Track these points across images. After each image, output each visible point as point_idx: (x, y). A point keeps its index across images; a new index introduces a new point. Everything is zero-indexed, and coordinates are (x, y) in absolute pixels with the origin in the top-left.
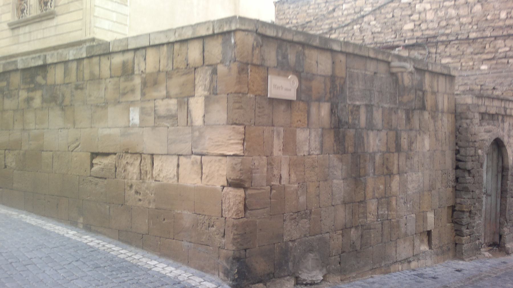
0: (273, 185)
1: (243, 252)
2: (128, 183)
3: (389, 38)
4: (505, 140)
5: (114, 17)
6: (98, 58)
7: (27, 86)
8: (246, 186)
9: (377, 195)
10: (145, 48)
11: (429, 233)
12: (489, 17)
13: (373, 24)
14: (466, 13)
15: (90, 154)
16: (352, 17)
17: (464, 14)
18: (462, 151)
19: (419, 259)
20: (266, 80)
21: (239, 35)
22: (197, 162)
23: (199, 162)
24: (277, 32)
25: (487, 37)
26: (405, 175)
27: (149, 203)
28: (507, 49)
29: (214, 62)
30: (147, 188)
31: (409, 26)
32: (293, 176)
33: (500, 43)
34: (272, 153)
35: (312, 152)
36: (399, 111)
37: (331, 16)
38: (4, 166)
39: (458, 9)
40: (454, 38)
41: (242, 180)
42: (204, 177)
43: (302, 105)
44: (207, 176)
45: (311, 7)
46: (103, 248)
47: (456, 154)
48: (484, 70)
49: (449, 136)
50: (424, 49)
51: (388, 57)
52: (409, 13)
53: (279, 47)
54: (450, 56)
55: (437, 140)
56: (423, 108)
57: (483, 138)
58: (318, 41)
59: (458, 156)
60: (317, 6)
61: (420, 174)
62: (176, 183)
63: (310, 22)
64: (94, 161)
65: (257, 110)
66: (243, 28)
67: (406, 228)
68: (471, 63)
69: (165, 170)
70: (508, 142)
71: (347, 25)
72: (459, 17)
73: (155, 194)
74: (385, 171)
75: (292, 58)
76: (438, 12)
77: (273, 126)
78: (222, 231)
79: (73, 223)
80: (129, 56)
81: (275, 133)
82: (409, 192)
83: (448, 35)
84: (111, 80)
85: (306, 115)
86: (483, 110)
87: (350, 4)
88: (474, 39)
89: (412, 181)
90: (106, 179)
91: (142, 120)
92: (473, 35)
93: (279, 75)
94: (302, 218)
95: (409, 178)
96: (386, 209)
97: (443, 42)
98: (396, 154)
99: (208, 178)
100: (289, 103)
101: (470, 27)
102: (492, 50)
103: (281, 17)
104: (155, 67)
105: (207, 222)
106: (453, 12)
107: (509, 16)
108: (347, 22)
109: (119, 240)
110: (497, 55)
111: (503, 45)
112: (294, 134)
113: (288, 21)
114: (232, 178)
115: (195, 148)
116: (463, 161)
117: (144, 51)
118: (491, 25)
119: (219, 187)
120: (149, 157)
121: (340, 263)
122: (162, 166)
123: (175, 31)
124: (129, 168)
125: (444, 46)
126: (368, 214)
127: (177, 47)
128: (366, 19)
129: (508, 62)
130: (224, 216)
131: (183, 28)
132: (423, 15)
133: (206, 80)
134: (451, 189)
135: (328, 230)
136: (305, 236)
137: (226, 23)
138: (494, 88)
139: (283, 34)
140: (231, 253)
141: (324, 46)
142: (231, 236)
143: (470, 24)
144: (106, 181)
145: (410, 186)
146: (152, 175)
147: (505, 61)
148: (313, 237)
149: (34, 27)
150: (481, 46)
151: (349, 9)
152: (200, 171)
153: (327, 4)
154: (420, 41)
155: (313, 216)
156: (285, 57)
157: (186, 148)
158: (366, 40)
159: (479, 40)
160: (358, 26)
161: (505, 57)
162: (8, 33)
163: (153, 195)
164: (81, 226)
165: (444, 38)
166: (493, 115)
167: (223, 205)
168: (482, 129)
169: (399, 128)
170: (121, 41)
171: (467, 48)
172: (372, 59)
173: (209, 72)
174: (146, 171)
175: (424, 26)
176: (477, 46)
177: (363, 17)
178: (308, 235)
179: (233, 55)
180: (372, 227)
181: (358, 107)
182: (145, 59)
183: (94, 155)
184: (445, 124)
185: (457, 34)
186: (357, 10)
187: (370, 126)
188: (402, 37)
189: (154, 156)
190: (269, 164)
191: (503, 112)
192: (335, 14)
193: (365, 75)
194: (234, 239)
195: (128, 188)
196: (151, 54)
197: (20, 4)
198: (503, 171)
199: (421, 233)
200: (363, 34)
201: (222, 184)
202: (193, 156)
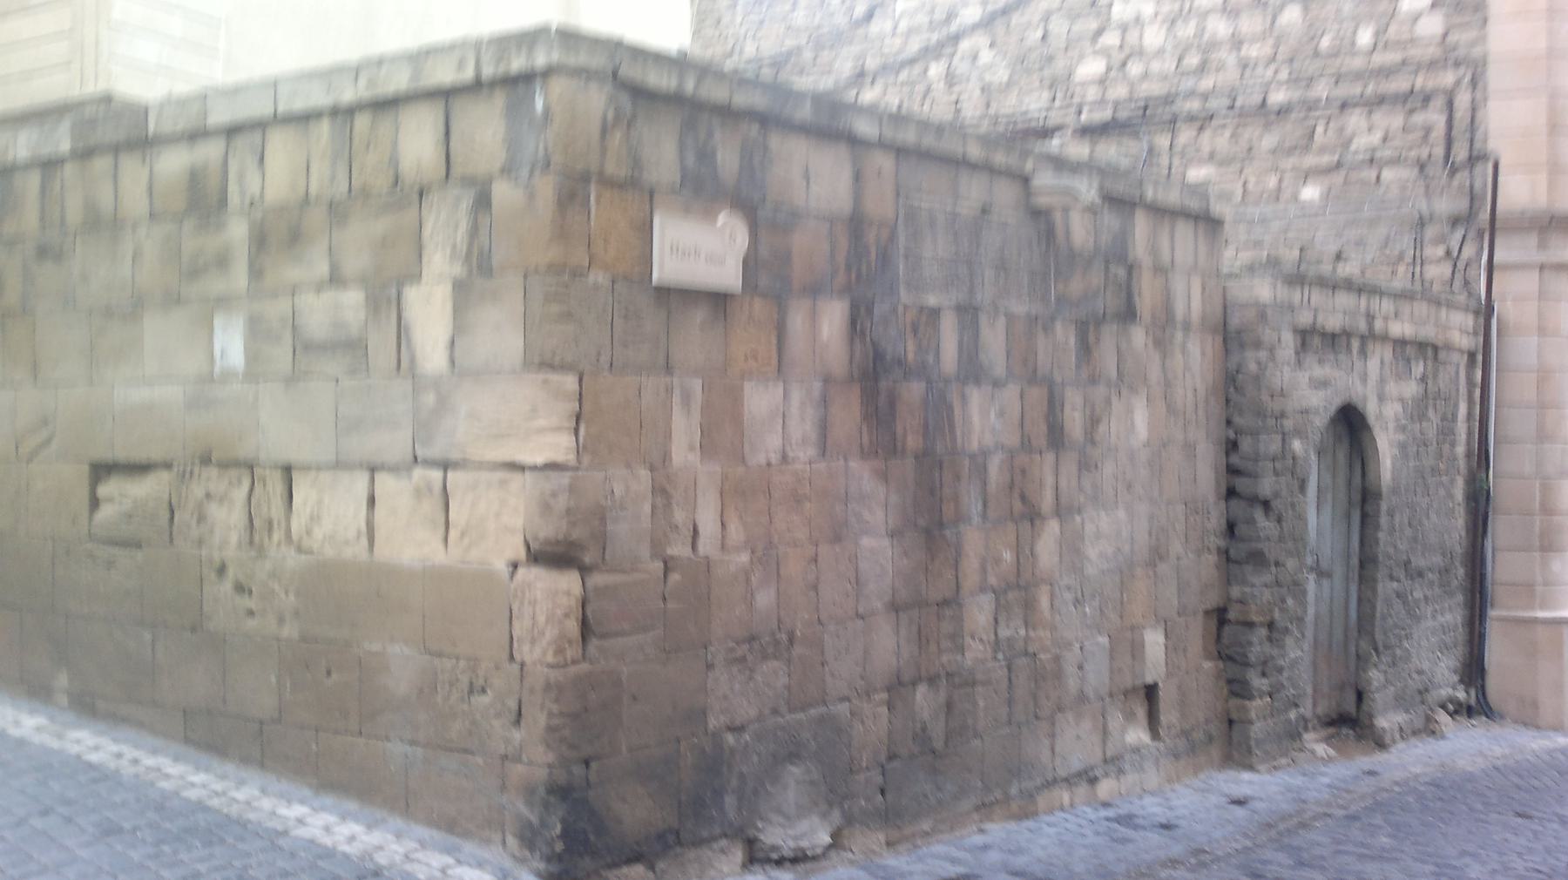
0: (672, 558)
1: (578, 770)
3: (1034, 103)
4: (1371, 409)
9: (992, 580)
10: (260, 126)
11: (1151, 692)
13: (986, 61)
15: (86, 468)
18: (1246, 444)
19: (1121, 772)
20: (646, 230)
21: (558, 86)
22: (430, 490)
23: (438, 486)
26: (1078, 519)
27: (281, 620)
30: (273, 575)
31: (1091, 68)
34: (666, 457)
35: (791, 454)
36: (1059, 327)
41: (572, 544)
42: (453, 534)
43: (759, 306)
44: (463, 534)
46: (132, 770)
47: (1227, 454)
49: (1207, 401)
50: (1136, 135)
53: (689, 126)
55: (1171, 409)
56: (1129, 314)
63: (799, 49)
64: (103, 490)
67: (1083, 679)
68: (1272, 182)
69: (329, 514)
70: (1380, 416)
74: (1018, 505)
75: (728, 159)
77: (668, 369)
79: (36, 691)
80: (211, 151)
81: (676, 399)
82: (1090, 571)
83: (1205, 97)
85: (774, 341)
86: (1305, 319)
89: (1098, 535)
90: (139, 546)
91: (252, 356)
92: (1278, 97)
93: (687, 210)
94: (765, 657)
95: (1090, 528)
96: (1020, 622)
97: (1191, 118)
98: (1050, 457)
99: (466, 541)
100: (719, 301)
105: (465, 679)
106: (1219, 27)
109: (187, 740)
112: (735, 398)
114: (542, 535)
116: (1249, 475)
117: (256, 137)
121: (883, 792)
122: (320, 502)
123: (356, 71)
124: (216, 512)
126: (968, 640)
127: (362, 122)
128: (965, 45)
131: (380, 62)
134: (1211, 559)
136: (775, 711)
139: (696, 87)
140: (541, 774)
141: (830, 124)
142: (542, 720)
145: (1092, 552)
146: (288, 531)
148: (800, 716)
154: (1123, 115)
155: (798, 650)
156: (706, 156)
157: (395, 444)
164: (63, 700)
165: (1194, 105)
166: (1334, 336)
167: (516, 623)
168: (1303, 378)
169: (1058, 378)
170: (182, 103)
173: (466, 203)
174: (270, 523)
175: (1135, 69)
176: (1290, 130)
178: (783, 709)
180: (979, 676)
181: (935, 313)
183: (102, 470)
184: (1195, 361)
187: (972, 370)
190: (661, 492)
191: (1362, 326)
193: (954, 217)
194: (550, 729)
195: (213, 576)
198: (1364, 500)
199: (1126, 693)
202: (418, 473)
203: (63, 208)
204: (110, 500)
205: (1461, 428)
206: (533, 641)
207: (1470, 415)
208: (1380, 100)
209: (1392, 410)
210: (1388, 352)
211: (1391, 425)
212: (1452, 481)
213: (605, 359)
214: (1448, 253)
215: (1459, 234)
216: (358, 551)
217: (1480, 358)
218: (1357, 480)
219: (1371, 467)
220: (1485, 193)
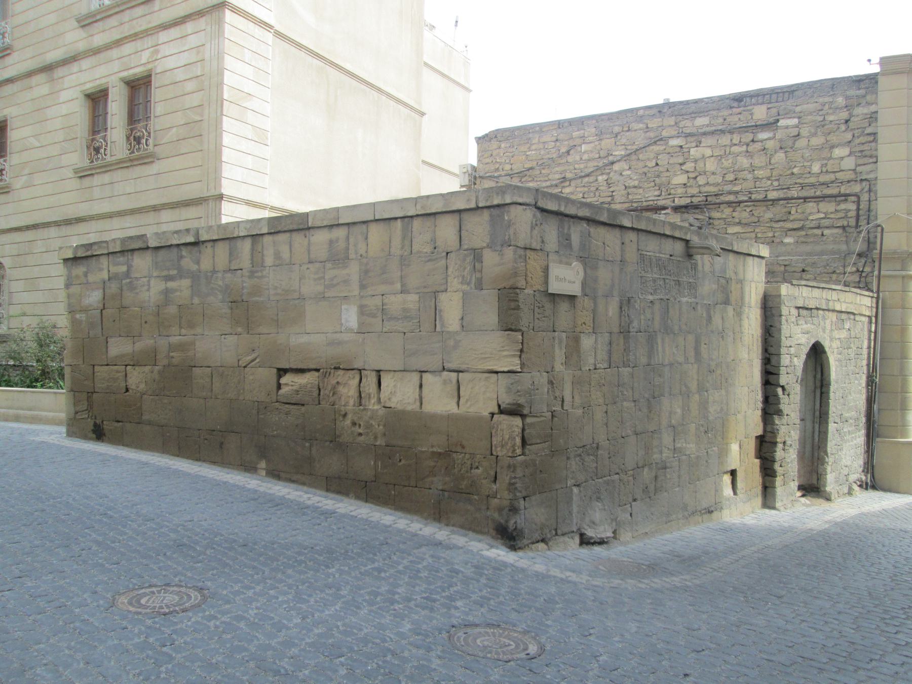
2: (340, 411)
3: (650, 195)
4: (826, 344)
5: (249, 161)
6: (288, 235)
7: (165, 273)
8: (525, 412)
12: (795, 171)
14: (763, 164)
16: (596, 164)
17: (760, 165)
20: (546, 270)
23: (454, 381)
24: (559, 205)
25: (793, 198)
27: (376, 438)
28: (822, 216)
29: (476, 246)
30: (371, 418)
31: (681, 179)
32: (577, 397)
33: (811, 206)
35: (598, 366)
36: (699, 307)
37: (564, 161)
38: (124, 390)
39: (752, 157)
40: (746, 198)
41: (519, 405)
42: (462, 401)
43: (587, 302)
45: (533, 147)
47: (765, 364)
48: (789, 244)
50: (703, 212)
51: (686, 233)
52: (681, 161)
54: (739, 223)
56: (727, 302)
57: (799, 342)
58: (606, 215)
59: (768, 367)
60: (541, 146)
61: (723, 392)
62: (418, 409)
63: (532, 168)
64: (283, 380)
65: (536, 309)
66: (520, 200)
68: (770, 234)
69: (399, 393)
70: (830, 347)
71: (588, 175)
72: (752, 169)
73: (384, 426)
74: (684, 389)
75: (575, 239)
76: (723, 160)
78: (493, 473)
79: (249, 468)
80: (341, 233)
81: (557, 341)
82: (711, 418)
83: (737, 193)
84: (310, 266)
87: (592, 145)
88: (773, 200)
90: (303, 405)
91: (361, 324)
92: (772, 195)
95: (711, 398)
97: (729, 203)
99: (469, 403)
100: (572, 298)
101: (769, 182)
102: (799, 217)
103: (488, 160)
104: (383, 250)
105: (469, 462)
106: (744, 162)
107: (824, 170)
108: (588, 171)
109: (328, 490)
110: (808, 222)
111: (815, 210)
112: (577, 340)
113: (497, 166)
115: (448, 362)
117: (364, 226)
118: (798, 181)
119: (486, 413)
120: (374, 373)
122: (395, 386)
124: (342, 390)
125: (731, 209)
127: (416, 223)
128: (616, 167)
129: (823, 235)
130: (494, 453)
132: (700, 165)
133: (465, 269)
134: (759, 413)
135: (618, 471)
137: (498, 194)
138: (803, 271)
139: (566, 207)
143: (768, 179)
144: (303, 408)
145: (711, 410)
146: (379, 399)
147: (818, 232)
148: (600, 480)
149: (119, 175)
150: (785, 210)
151: (592, 152)
152: (456, 394)
153: (558, 144)
154: (696, 200)
155: (600, 452)
156: (568, 238)
157: (434, 362)
158: (616, 197)
159: (782, 202)
160: (605, 177)
161: (818, 227)
162: (74, 183)
163: (381, 427)
165: (731, 198)
167: (494, 439)
170: (325, 211)
171: (765, 212)
172: (668, 236)
173: (470, 259)
174: (369, 394)
175: (701, 180)
177: (613, 163)
178: (594, 478)
179: (507, 237)
180: (668, 465)
182: (366, 238)
183: (282, 372)
185: (750, 193)
186: (603, 154)
187: (667, 330)
188: (670, 194)
189: (382, 373)
190: (551, 383)
191: (824, 307)
192: (570, 159)
193: (660, 259)
195: (341, 419)
196: (375, 232)
197: (93, 140)
198: (822, 386)
200: (611, 189)
201: (491, 410)
202: (445, 373)
203: (263, 255)
204: (286, 384)
205: (865, 352)
206: (502, 446)
207: (869, 347)
208: (824, 197)
209: (835, 344)
210: (834, 319)
211: (836, 350)
212: (861, 377)
213: (531, 325)
214: (858, 271)
215: (863, 260)
216: (413, 407)
217: (874, 319)
218: (819, 376)
219: (825, 370)
220: (875, 243)
